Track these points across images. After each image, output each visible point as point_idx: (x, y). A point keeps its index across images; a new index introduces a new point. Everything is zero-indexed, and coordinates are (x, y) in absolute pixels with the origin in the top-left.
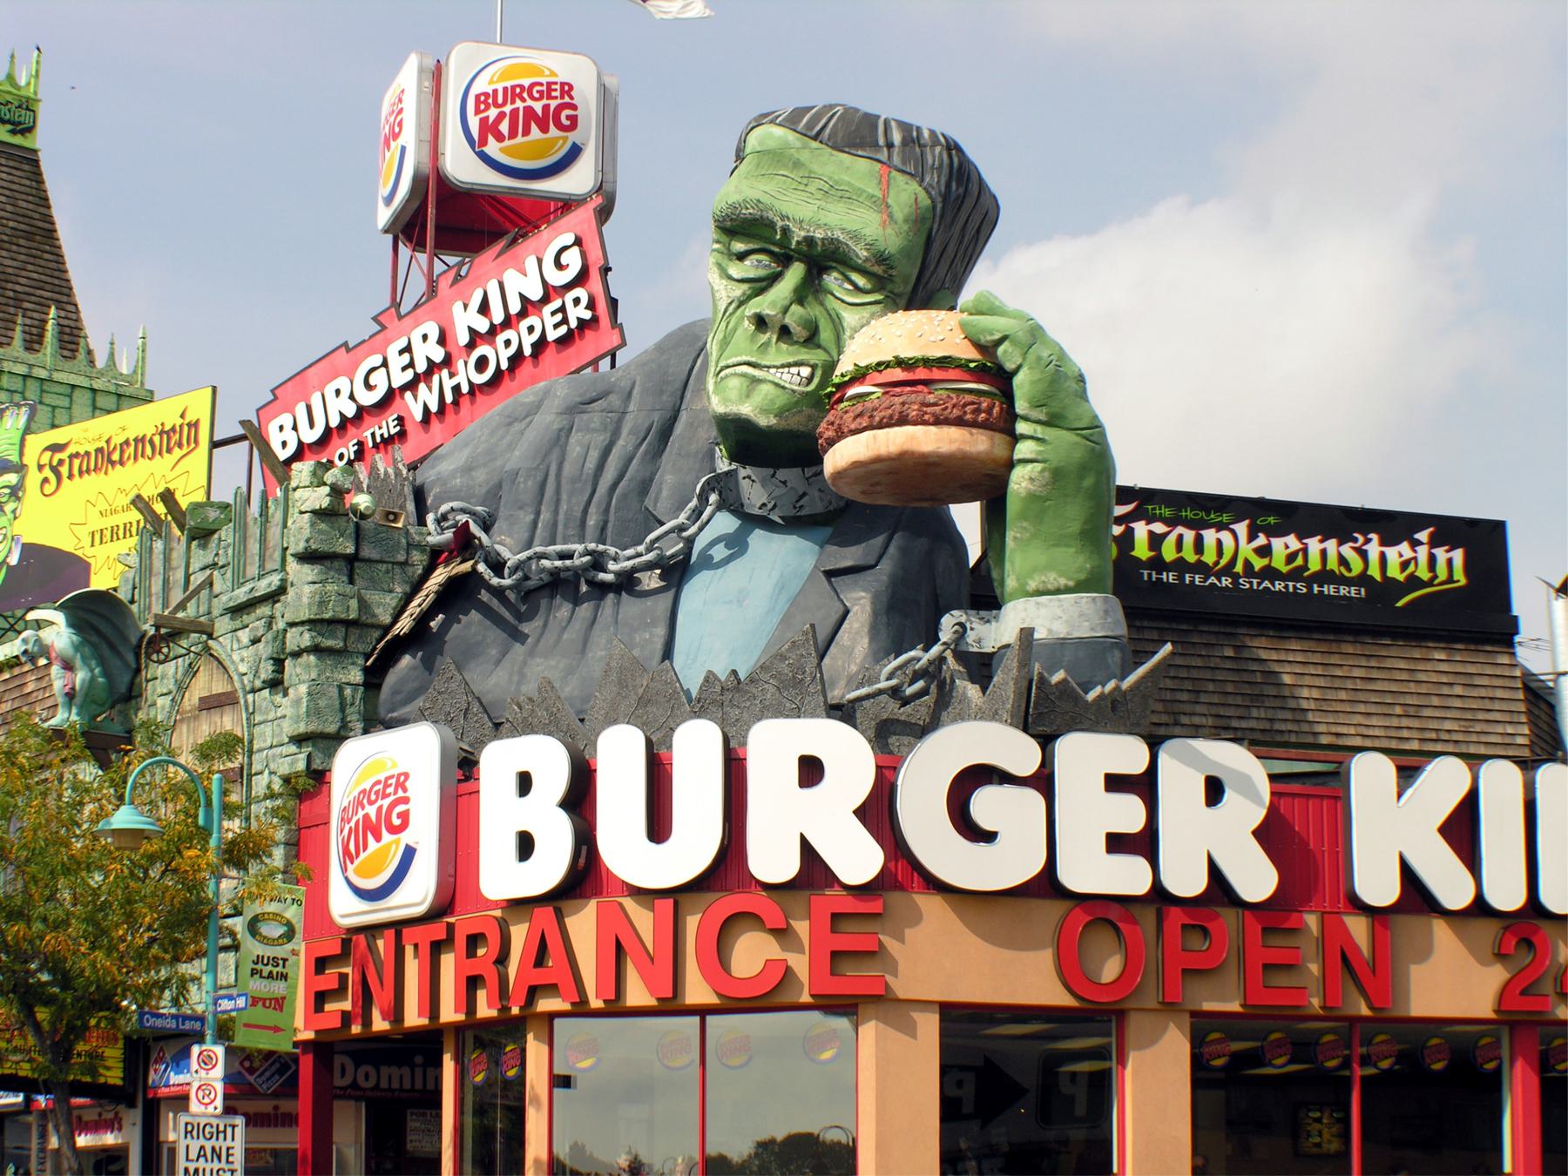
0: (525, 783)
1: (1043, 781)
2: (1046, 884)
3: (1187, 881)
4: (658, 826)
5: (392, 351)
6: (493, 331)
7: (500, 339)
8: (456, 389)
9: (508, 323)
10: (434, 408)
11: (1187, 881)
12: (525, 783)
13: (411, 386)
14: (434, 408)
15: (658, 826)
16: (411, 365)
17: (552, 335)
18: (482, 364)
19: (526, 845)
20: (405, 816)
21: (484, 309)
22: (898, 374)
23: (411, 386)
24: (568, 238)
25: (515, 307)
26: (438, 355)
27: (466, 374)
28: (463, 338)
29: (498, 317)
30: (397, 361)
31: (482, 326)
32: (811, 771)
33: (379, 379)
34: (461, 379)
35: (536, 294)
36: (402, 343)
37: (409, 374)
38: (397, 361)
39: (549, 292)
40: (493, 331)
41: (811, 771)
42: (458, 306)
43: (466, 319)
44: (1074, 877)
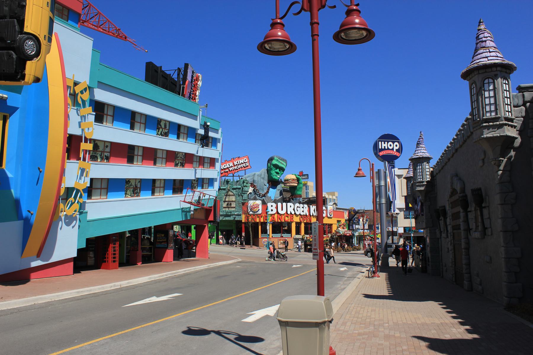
0: (272, 206)
1: (300, 207)
2: (300, 214)
3: (305, 214)
4: (282, 210)
5: (227, 164)
6: (238, 165)
7: (239, 165)
8: (235, 169)
9: (240, 164)
10: (232, 170)
11: (305, 214)
12: (272, 206)
13: (230, 167)
14: (232, 170)
15: (282, 210)
16: (229, 166)
17: (245, 166)
18: (237, 167)
19: (272, 210)
20: (259, 207)
21: (237, 162)
22: (292, 180)
23: (230, 167)
24: (246, 159)
25: (241, 163)
26: (233, 165)
27: (236, 167)
28: (235, 165)
29: (239, 163)
30: (228, 165)
31: (237, 164)
32: (291, 206)
33: (226, 166)
34: (235, 168)
35: (243, 162)
36: (229, 164)
37: (229, 167)
38: (228, 165)
39: (244, 163)
40: (238, 165)
41: (291, 206)
42: (234, 162)
43: (235, 163)
44: (301, 214)
